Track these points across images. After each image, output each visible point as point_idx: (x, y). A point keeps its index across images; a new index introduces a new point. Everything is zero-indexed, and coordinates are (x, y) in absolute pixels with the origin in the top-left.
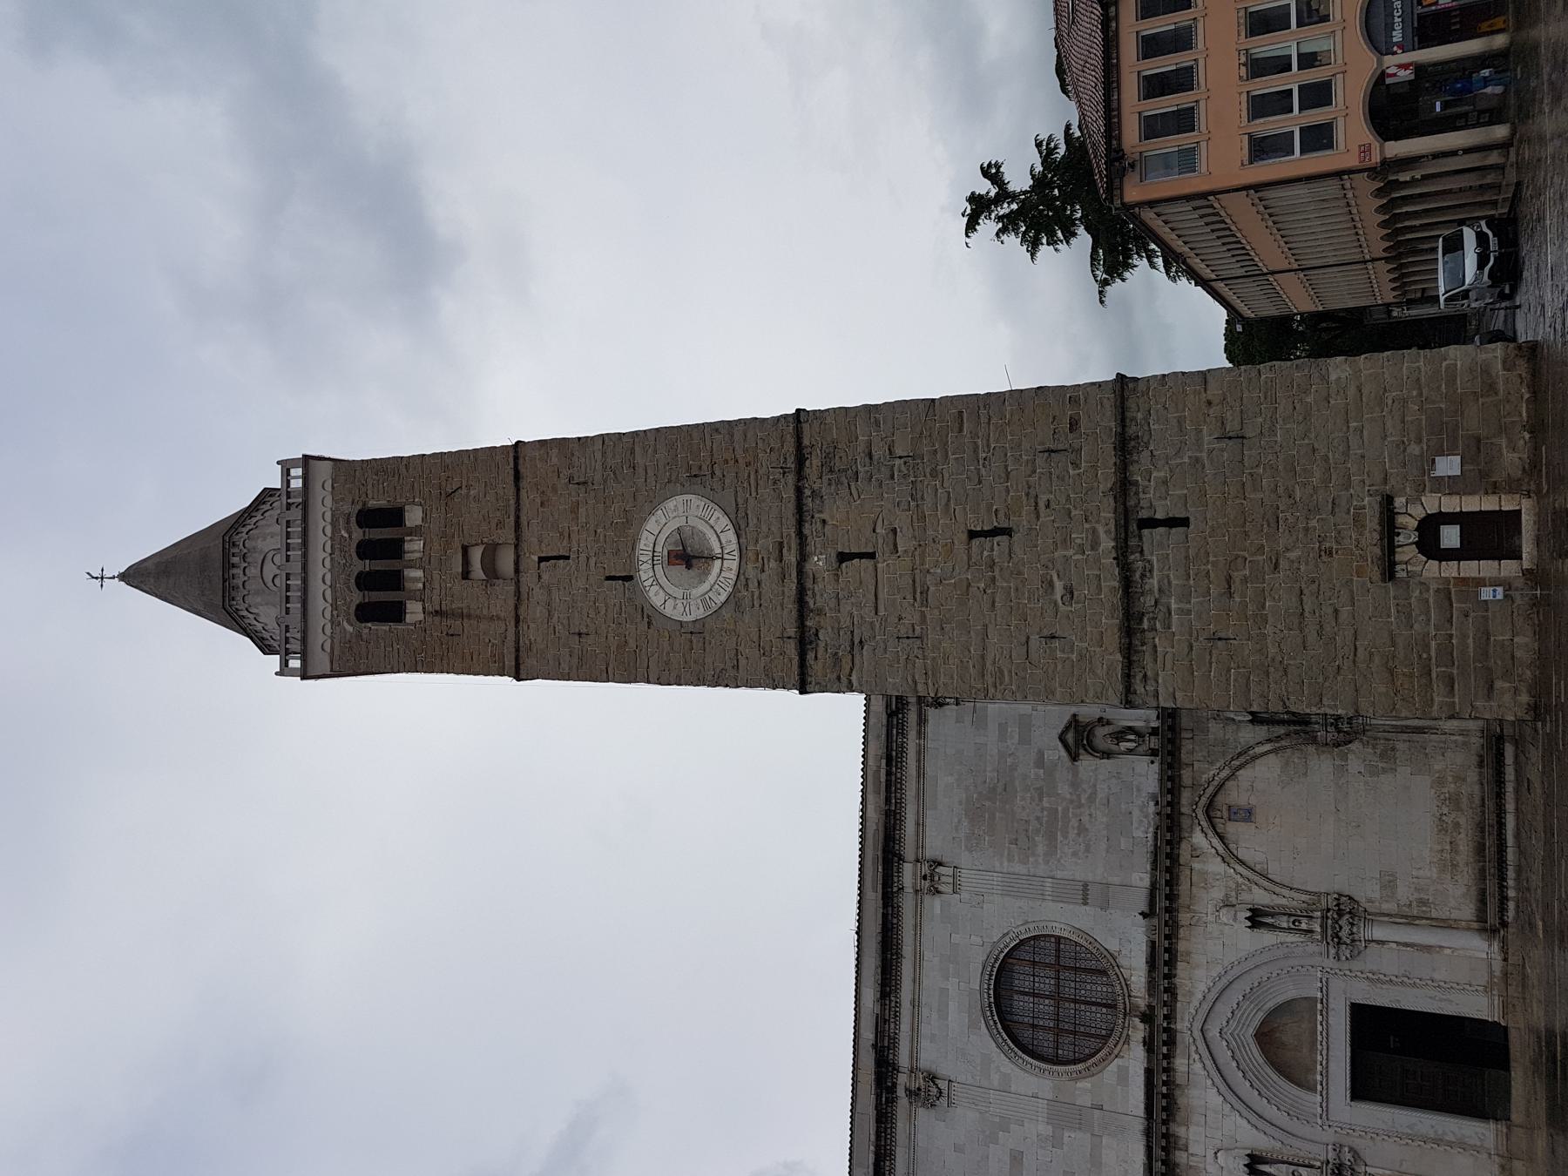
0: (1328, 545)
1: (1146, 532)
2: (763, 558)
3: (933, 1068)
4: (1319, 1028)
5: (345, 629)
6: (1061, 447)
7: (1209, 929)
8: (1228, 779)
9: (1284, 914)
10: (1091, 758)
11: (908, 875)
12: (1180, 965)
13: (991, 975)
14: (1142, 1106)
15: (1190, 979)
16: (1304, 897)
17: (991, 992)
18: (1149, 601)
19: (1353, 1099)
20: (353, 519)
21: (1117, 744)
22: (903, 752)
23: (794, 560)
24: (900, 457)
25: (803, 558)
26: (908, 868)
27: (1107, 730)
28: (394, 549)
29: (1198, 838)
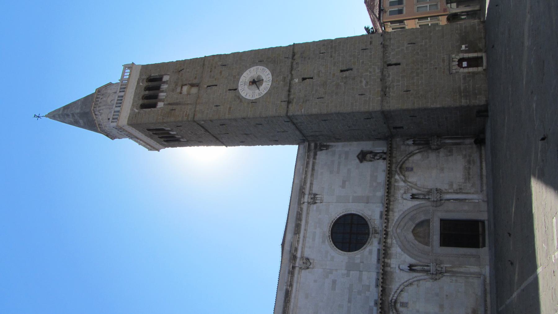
0: (435, 67)
1: (389, 67)
2: (279, 81)
3: (309, 257)
4: (431, 226)
5: (135, 111)
6: (367, 48)
7: (399, 201)
8: (406, 160)
9: (421, 195)
10: (365, 162)
11: (306, 198)
12: (391, 213)
13: (330, 227)
14: (376, 261)
15: (393, 216)
16: (427, 190)
17: (330, 232)
18: (388, 84)
19: (441, 246)
20: (145, 80)
21: (374, 158)
22: (308, 163)
23: (289, 81)
24: (322, 53)
25: (292, 79)
26: (306, 196)
27: (371, 154)
28: (158, 88)
29: (397, 177)
